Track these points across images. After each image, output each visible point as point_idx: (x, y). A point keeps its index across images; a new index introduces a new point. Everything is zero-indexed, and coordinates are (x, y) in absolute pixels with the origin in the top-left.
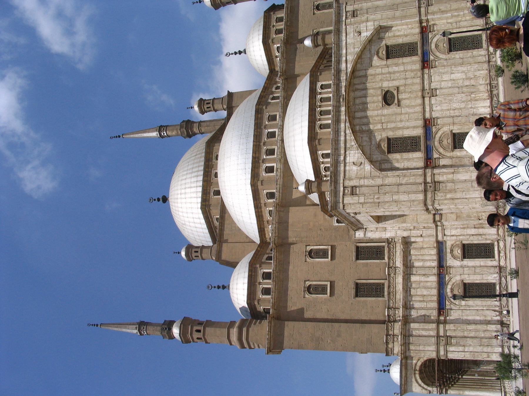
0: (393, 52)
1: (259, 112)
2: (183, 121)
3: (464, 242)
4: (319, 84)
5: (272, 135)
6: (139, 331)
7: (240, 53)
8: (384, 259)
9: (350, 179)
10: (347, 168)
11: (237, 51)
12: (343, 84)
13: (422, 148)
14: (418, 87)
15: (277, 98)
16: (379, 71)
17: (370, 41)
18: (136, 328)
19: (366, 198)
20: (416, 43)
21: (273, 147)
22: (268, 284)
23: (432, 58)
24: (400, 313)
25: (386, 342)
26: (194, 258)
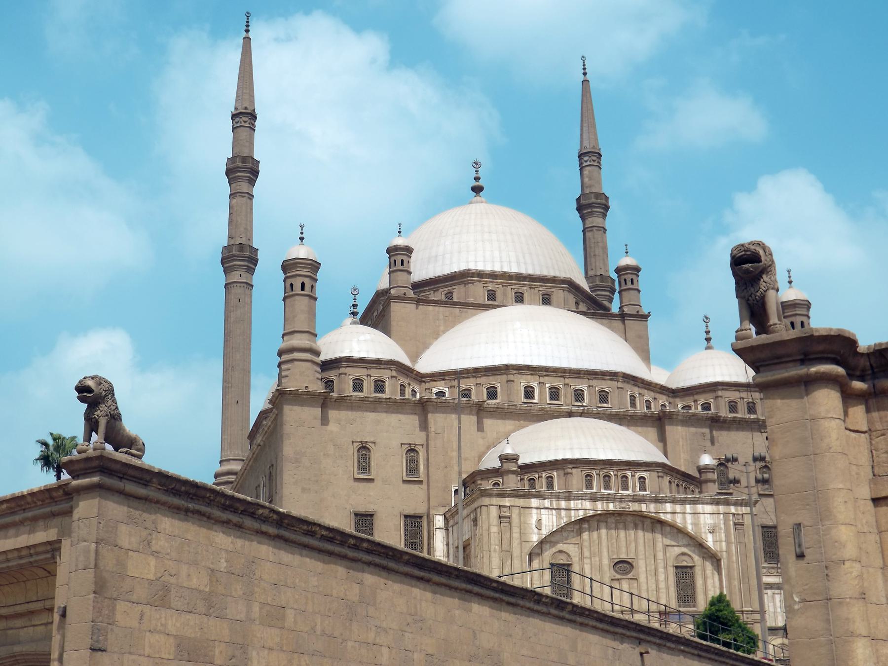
1: (613, 375)
2: (607, 198)
4: (644, 474)
5: (579, 395)
6: (241, 113)
7: (708, 340)
9: (520, 514)
10: (534, 511)
11: (711, 335)
12: (644, 507)
15: (633, 404)
16: (660, 555)
18: (246, 108)
20: (694, 606)
21: (562, 398)
26: (393, 259)
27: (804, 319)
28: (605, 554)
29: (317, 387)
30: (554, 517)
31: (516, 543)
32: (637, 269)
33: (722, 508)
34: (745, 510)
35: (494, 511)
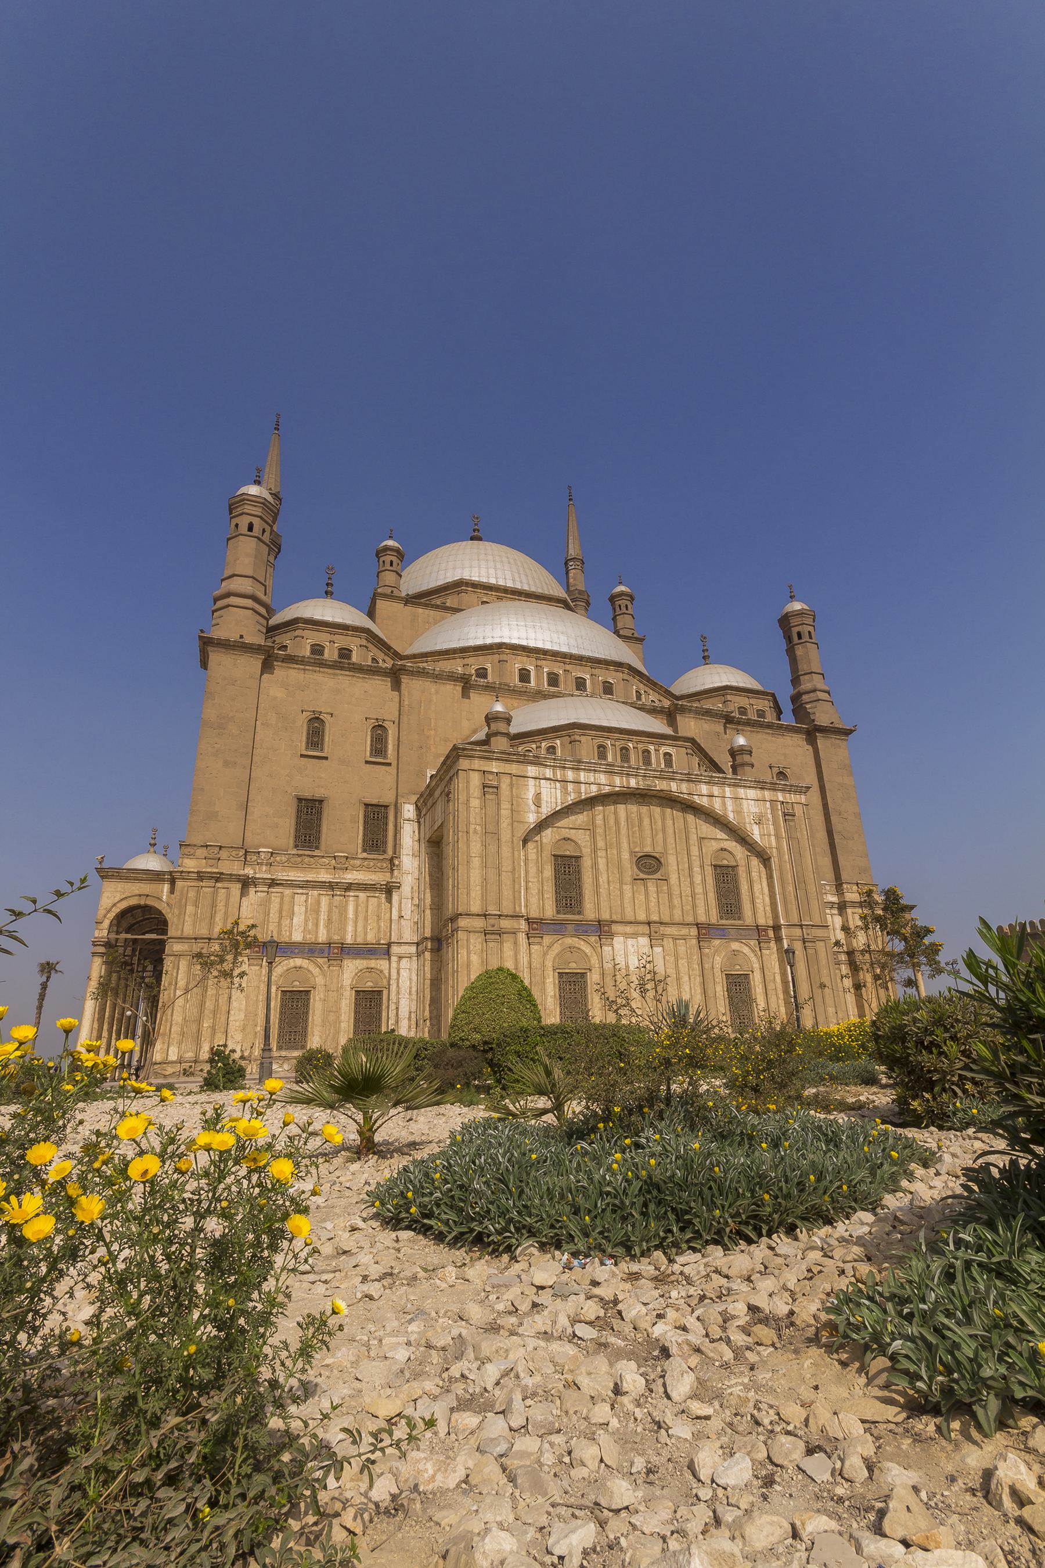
0: (726, 878)
1: (618, 665)
3: (385, 993)
4: (669, 750)
5: (580, 684)
8: (364, 851)
9: (511, 785)
10: (531, 782)
12: (674, 786)
13: (562, 916)
14: (666, 919)
16: (695, 851)
17: (743, 839)
19: (477, 810)
21: (562, 685)
22: (330, 654)
23: (717, 942)
24: (263, 873)
25: (207, 846)
26: (382, 559)
27: (811, 629)
28: (625, 845)
29: (259, 640)
30: (558, 792)
31: (505, 823)
32: (632, 598)
33: (767, 794)
34: (793, 798)
35: (475, 779)
